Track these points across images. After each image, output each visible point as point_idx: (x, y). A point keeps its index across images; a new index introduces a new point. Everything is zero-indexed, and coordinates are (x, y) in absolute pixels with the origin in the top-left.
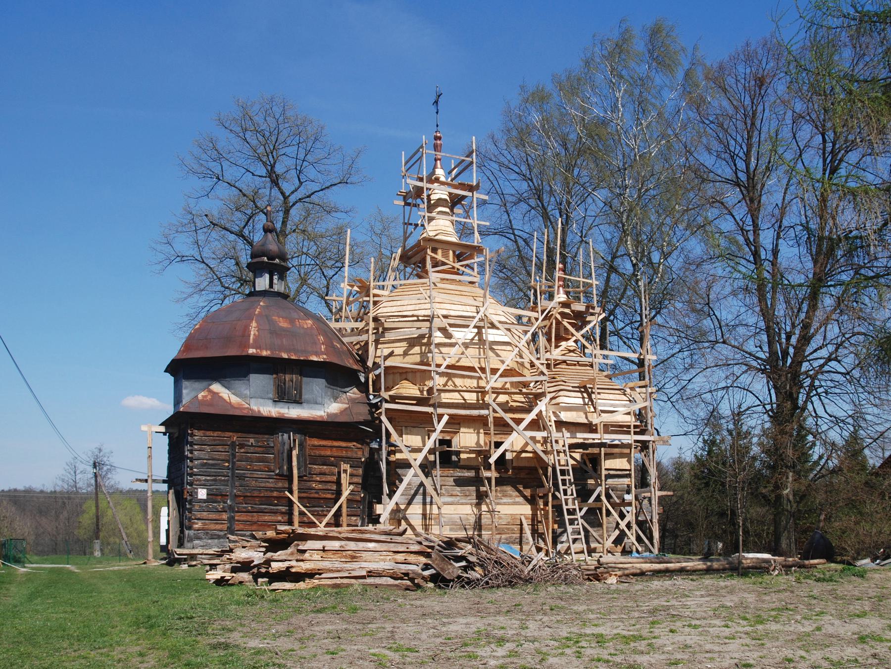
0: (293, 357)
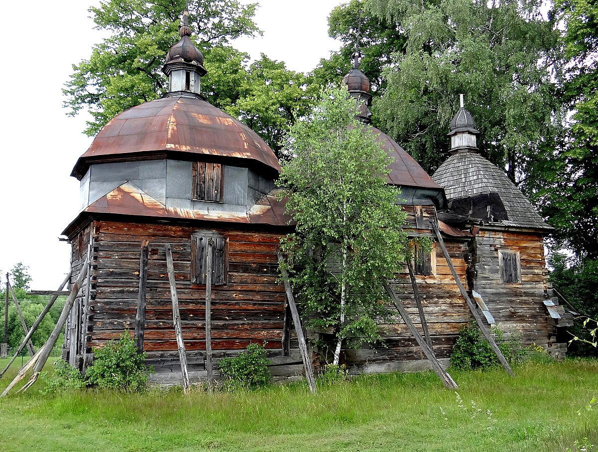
0: (215, 154)
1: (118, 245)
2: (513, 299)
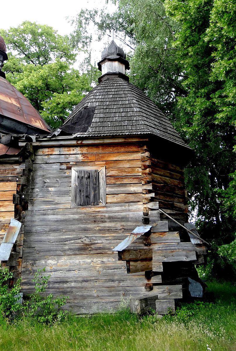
2: (89, 226)
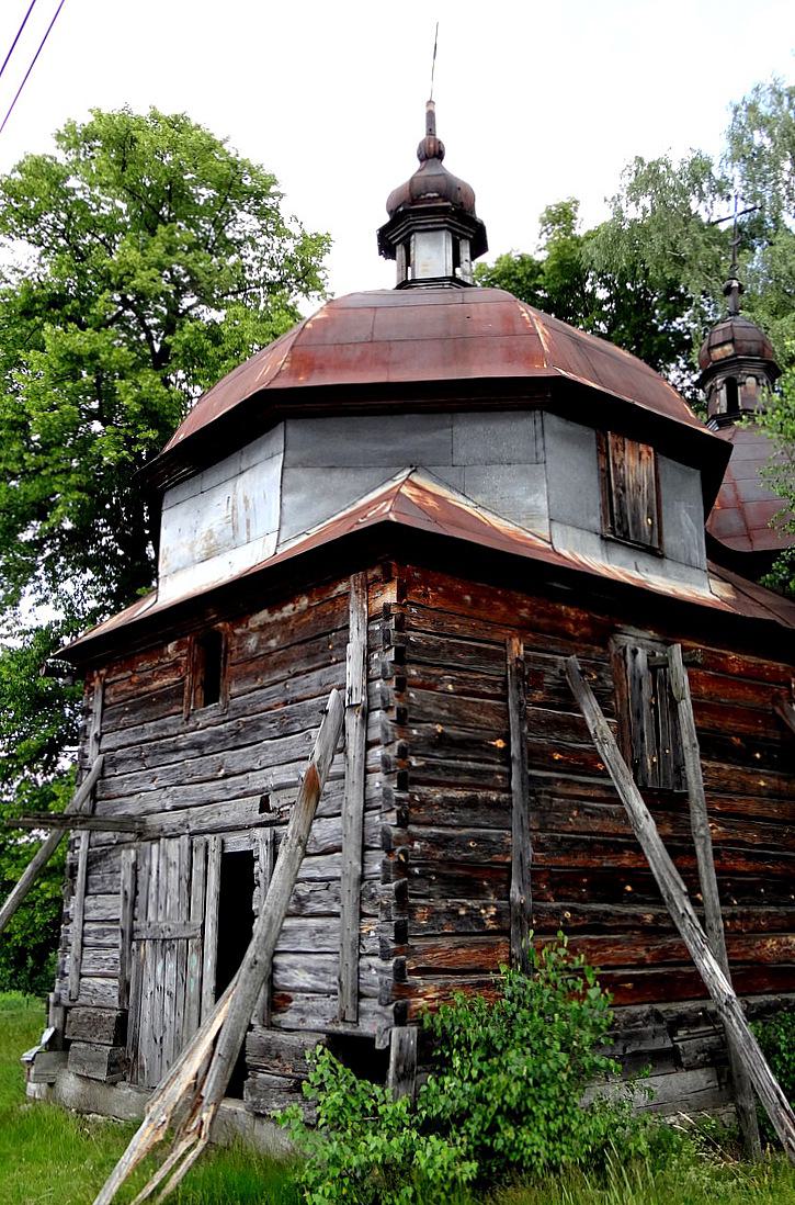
1: (452, 649)
